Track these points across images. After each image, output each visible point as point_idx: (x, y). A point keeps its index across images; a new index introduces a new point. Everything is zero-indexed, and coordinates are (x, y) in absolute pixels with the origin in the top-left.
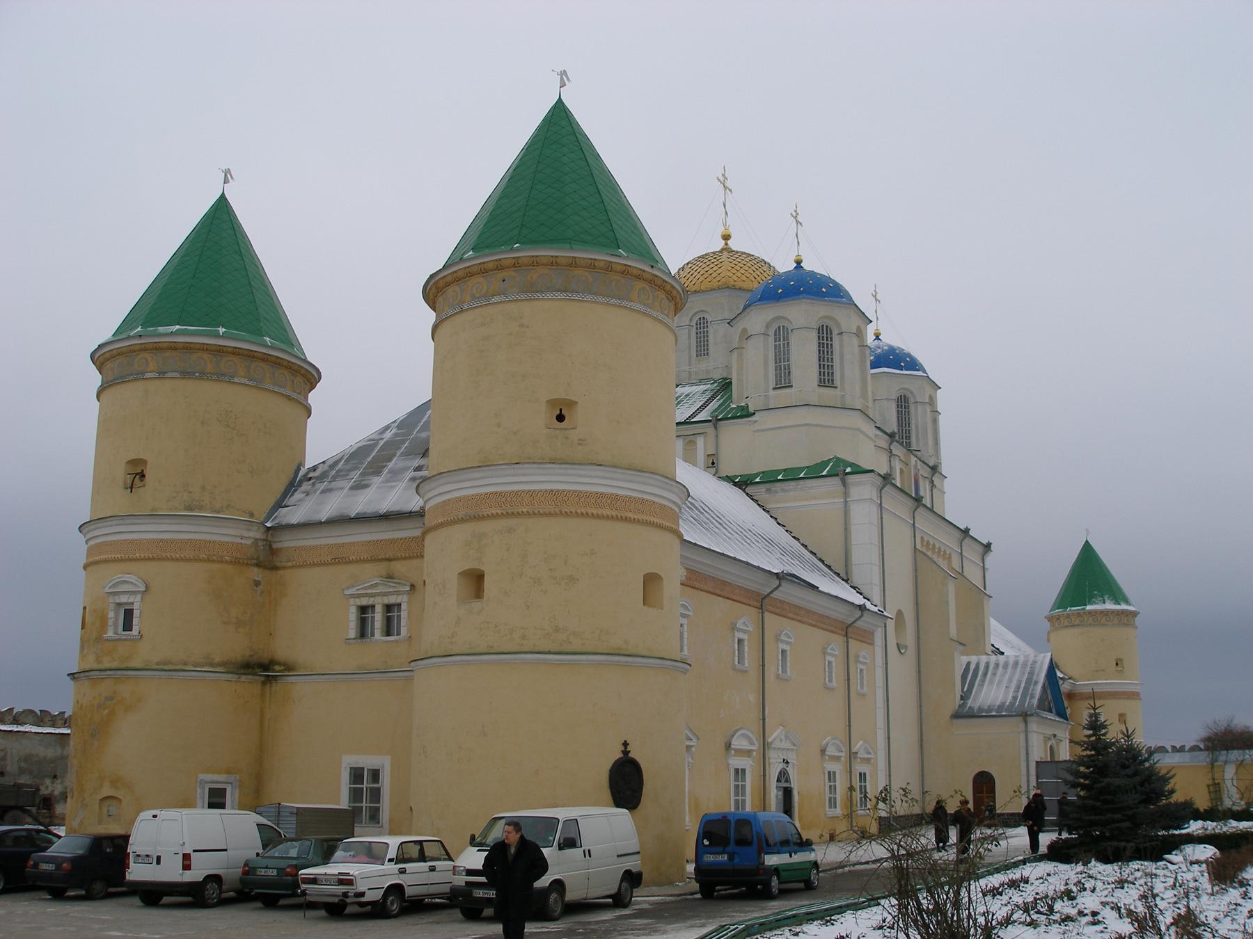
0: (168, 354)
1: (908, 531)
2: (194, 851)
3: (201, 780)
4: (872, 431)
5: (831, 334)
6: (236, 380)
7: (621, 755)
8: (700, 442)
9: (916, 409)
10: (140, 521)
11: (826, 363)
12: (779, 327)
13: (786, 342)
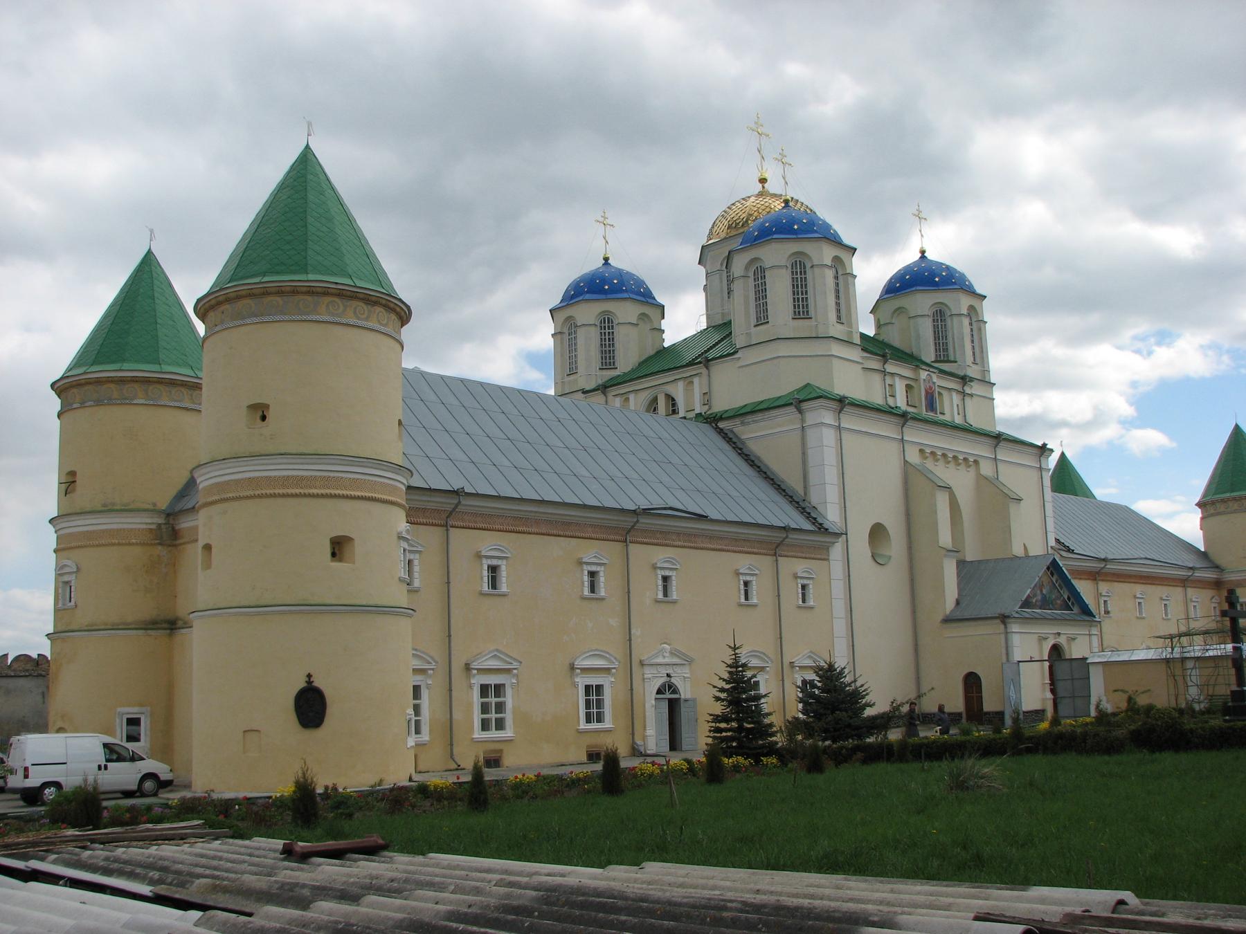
0: (86, 388)
1: (894, 447)
2: (33, 765)
3: (119, 712)
4: (855, 354)
5: (805, 267)
6: (135, 402)
7: (305, 685)
8: (696, 380)
9: (952, 320)
10: (73, 519)
11: (800, 296)
13: (763, 281)
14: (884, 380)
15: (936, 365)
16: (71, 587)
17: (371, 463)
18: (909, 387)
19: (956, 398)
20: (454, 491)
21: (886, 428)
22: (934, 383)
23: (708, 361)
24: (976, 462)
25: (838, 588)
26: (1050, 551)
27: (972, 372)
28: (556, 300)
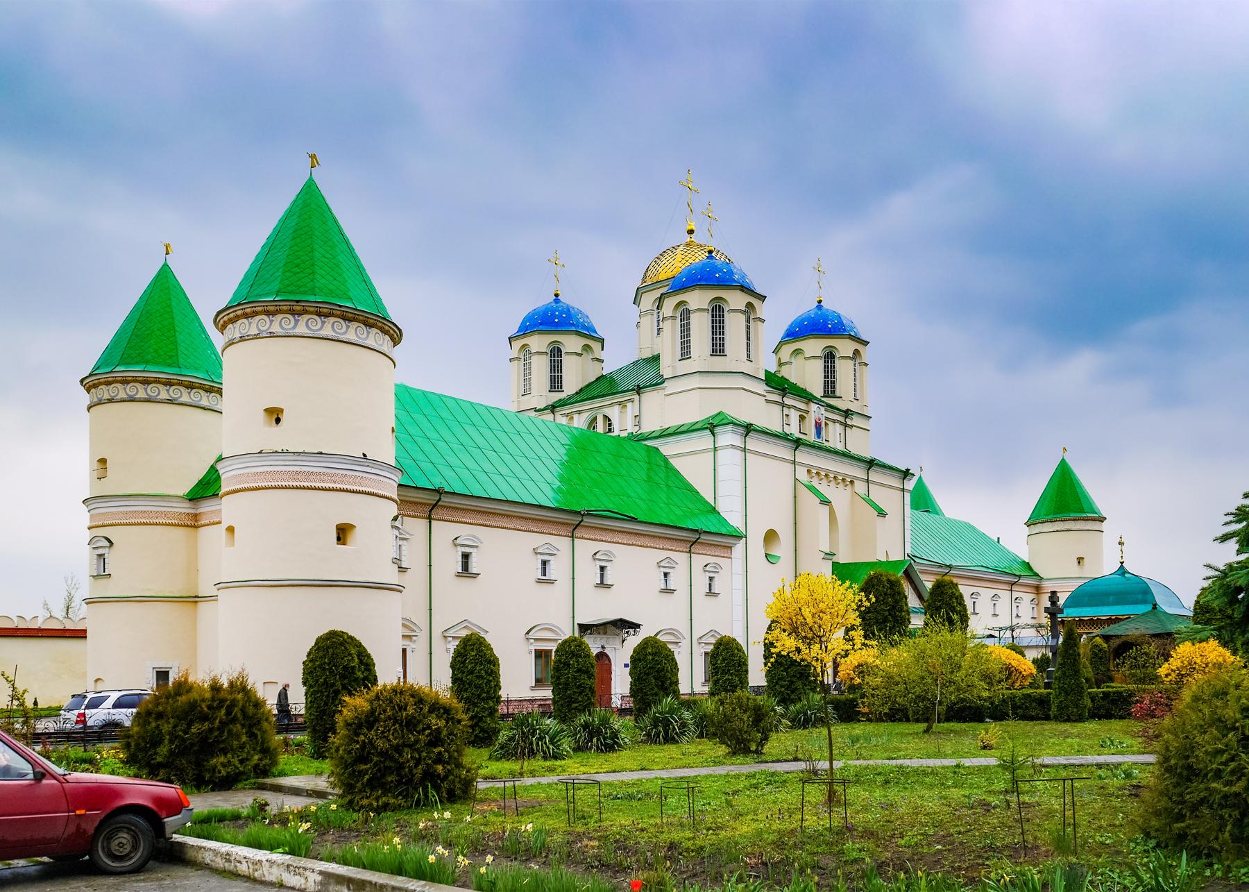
4: (761, 388)
8: (629, 405)
14: (783, 410)
15: (823, 399)
16: (104, 559)
18: (802, 418)
19: (839, 428)
20: (435, 490)
21: (784, 451)
22: (822, 414)
24: (852, 482)
27: (854, 407)
28: (513, 329)
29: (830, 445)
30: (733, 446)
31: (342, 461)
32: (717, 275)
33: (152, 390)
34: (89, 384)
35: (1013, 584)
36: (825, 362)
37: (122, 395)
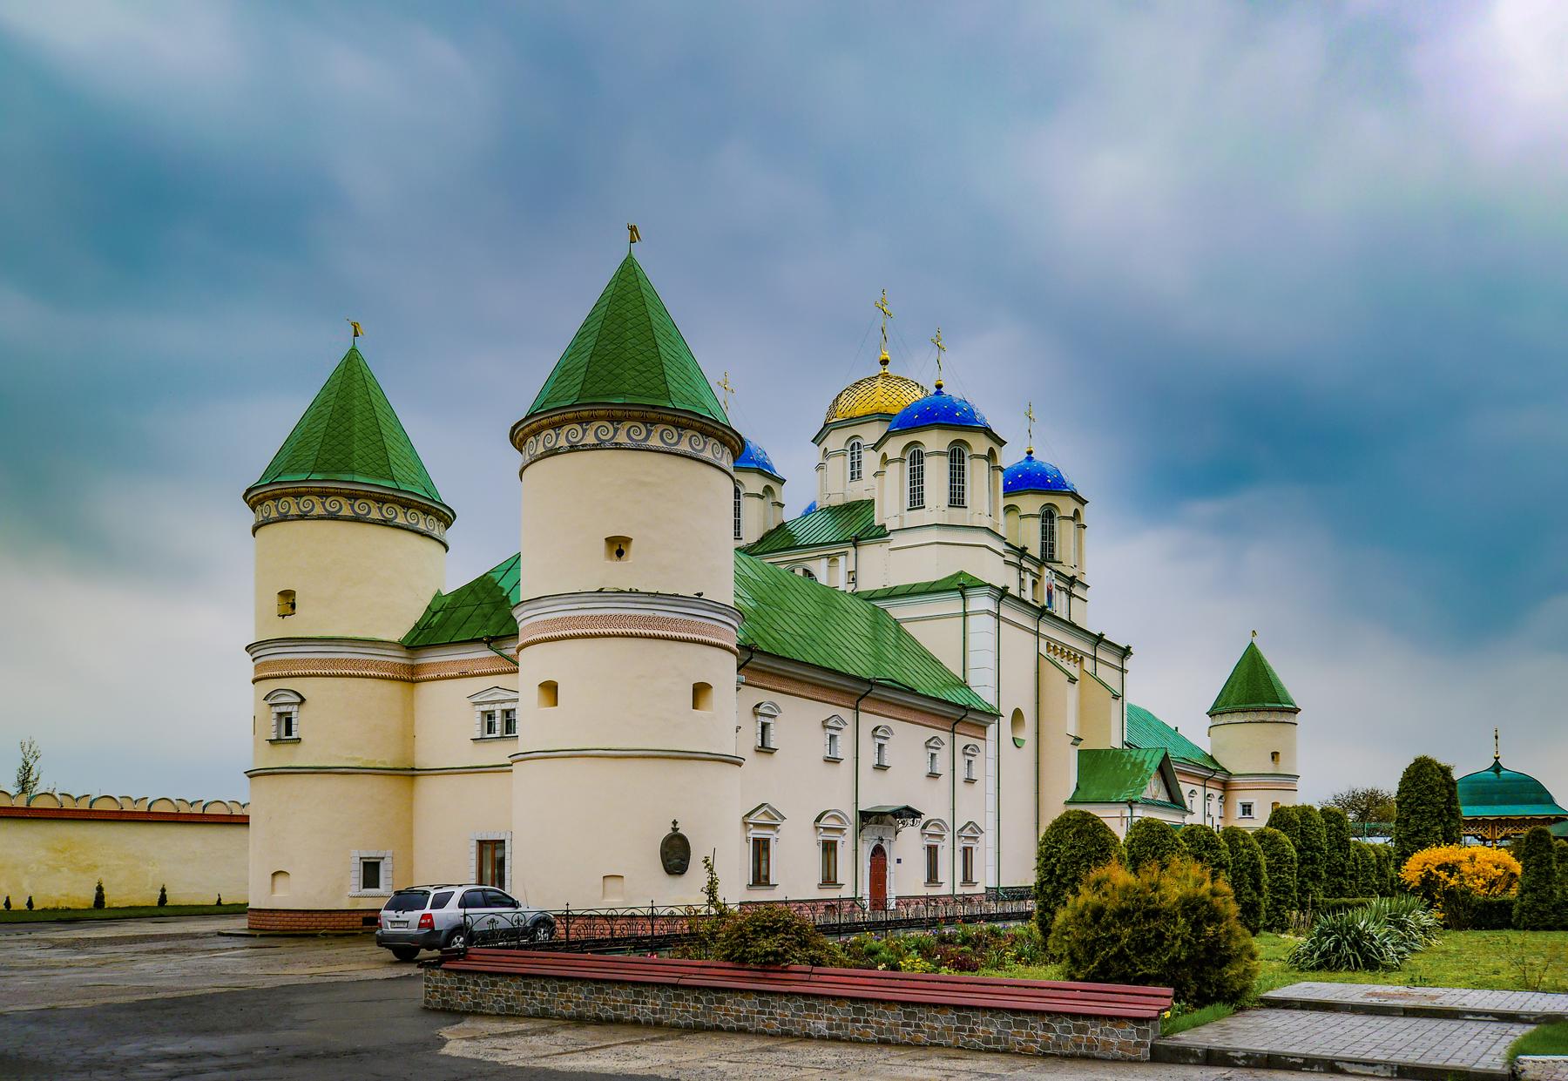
1: (1033, 638)
4: (1000, 547)
5: (963, 456)
8: (842, 559)
11: (957, 484)
12: (915, 451)
14: (1020, 574)
17: (728, 610)
18: (1034, 583)
23: (856, 542)
24: (1081, 658)
25: (992, 769)
26: (1125, 747)
29: (1056, 614)
30: (989, 612)
31: (703, 606)
32: (957, 414)
33: (360, 508)
34: (254, 497)
35: (1206, 779)
36: (1043, 522)
37: (318, 510)
